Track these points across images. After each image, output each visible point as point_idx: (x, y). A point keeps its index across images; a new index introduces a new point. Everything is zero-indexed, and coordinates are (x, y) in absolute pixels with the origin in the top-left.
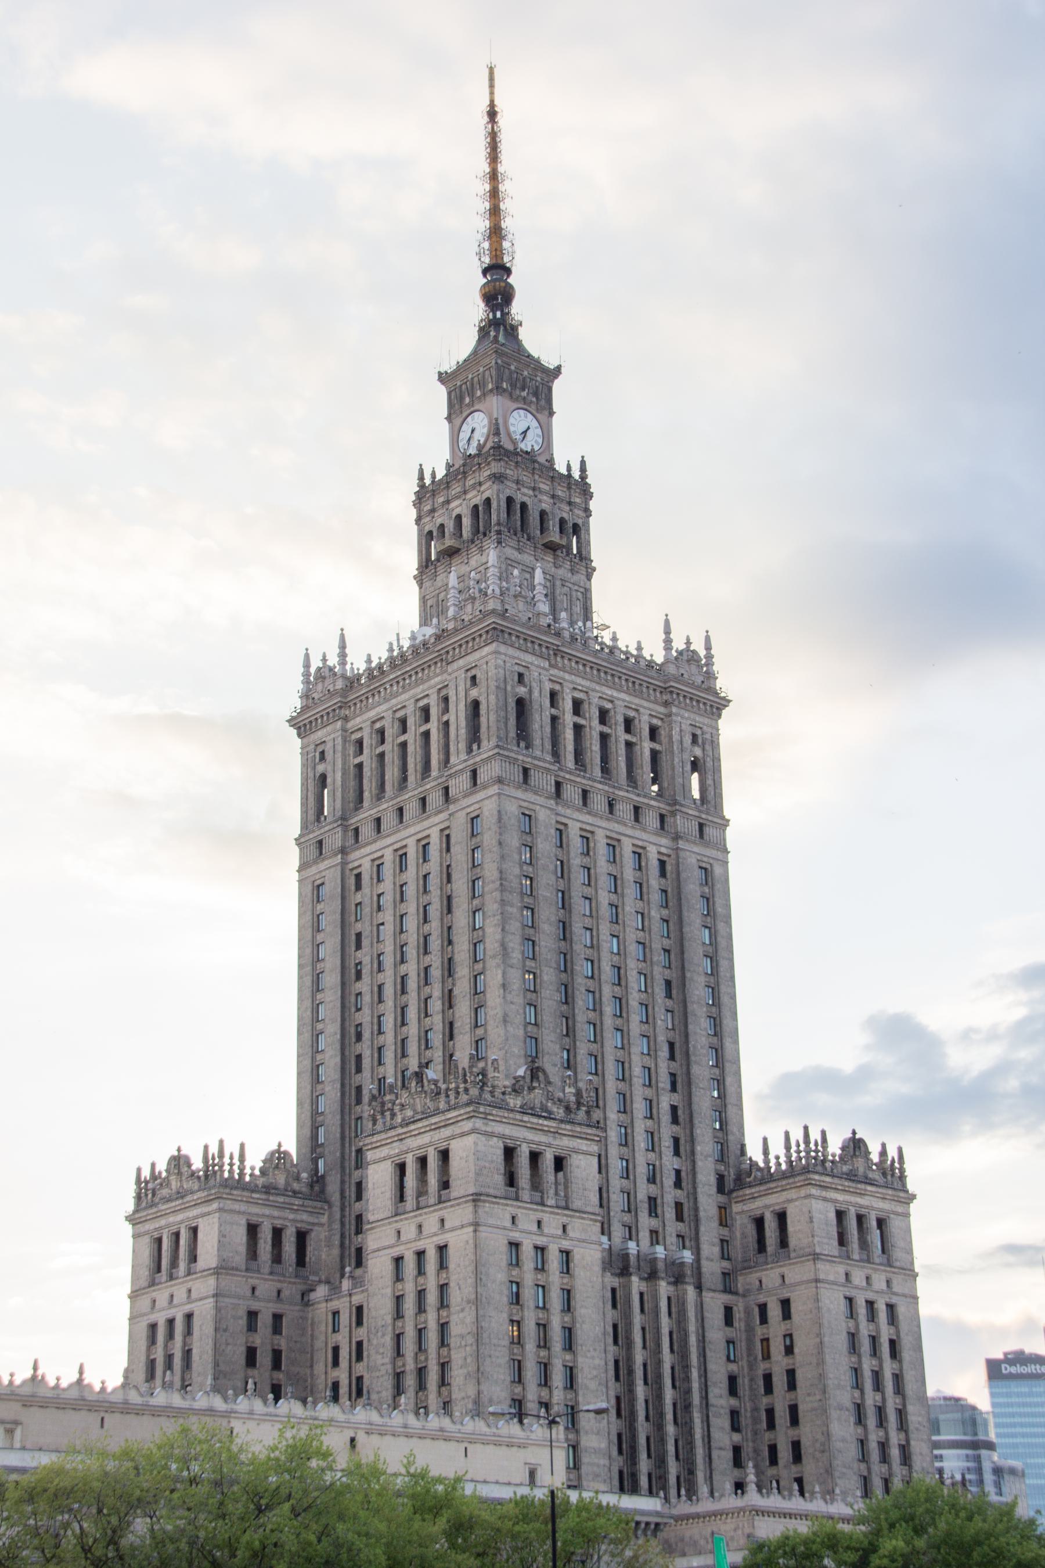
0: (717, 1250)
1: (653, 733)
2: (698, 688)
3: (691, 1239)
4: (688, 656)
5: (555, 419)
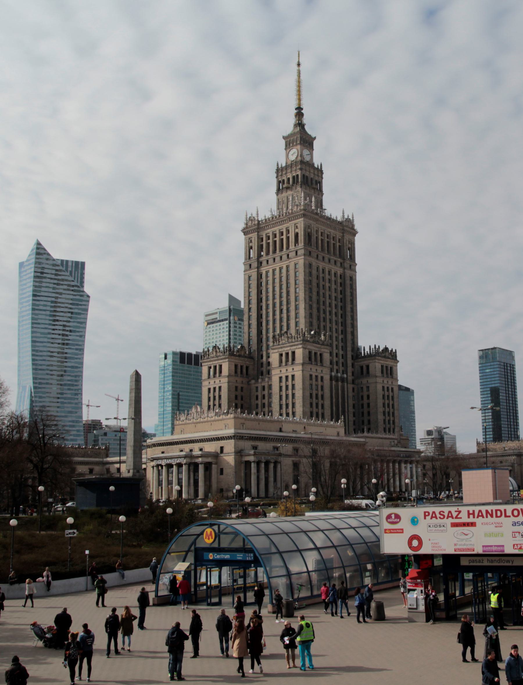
0: (351, 374)
2: (350, 228)
3: (345, 372)
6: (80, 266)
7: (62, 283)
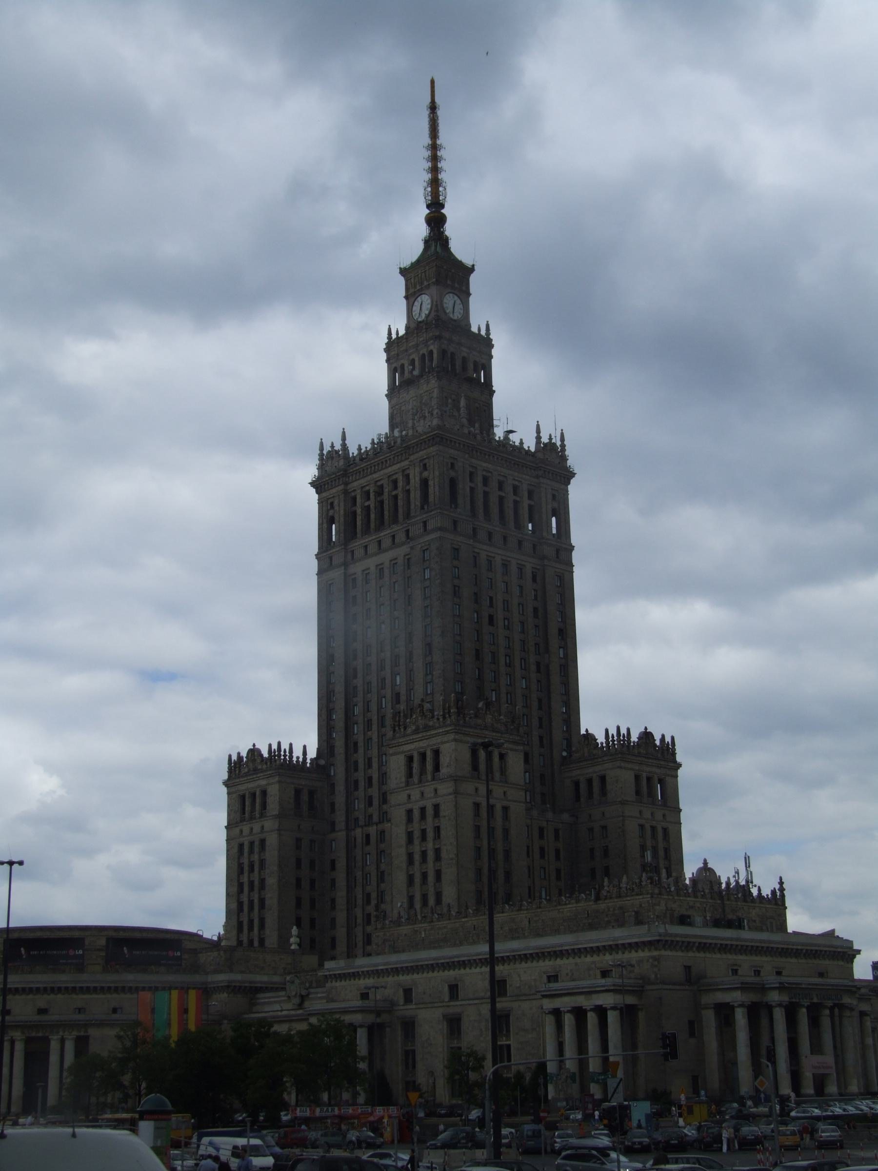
1: (530, 496)
4: (550, 446)
5: (471, 299)
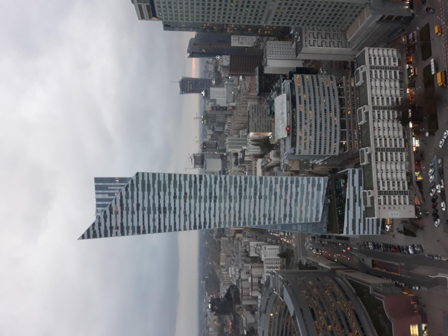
6: (101, 184)
7: (125, 206)
